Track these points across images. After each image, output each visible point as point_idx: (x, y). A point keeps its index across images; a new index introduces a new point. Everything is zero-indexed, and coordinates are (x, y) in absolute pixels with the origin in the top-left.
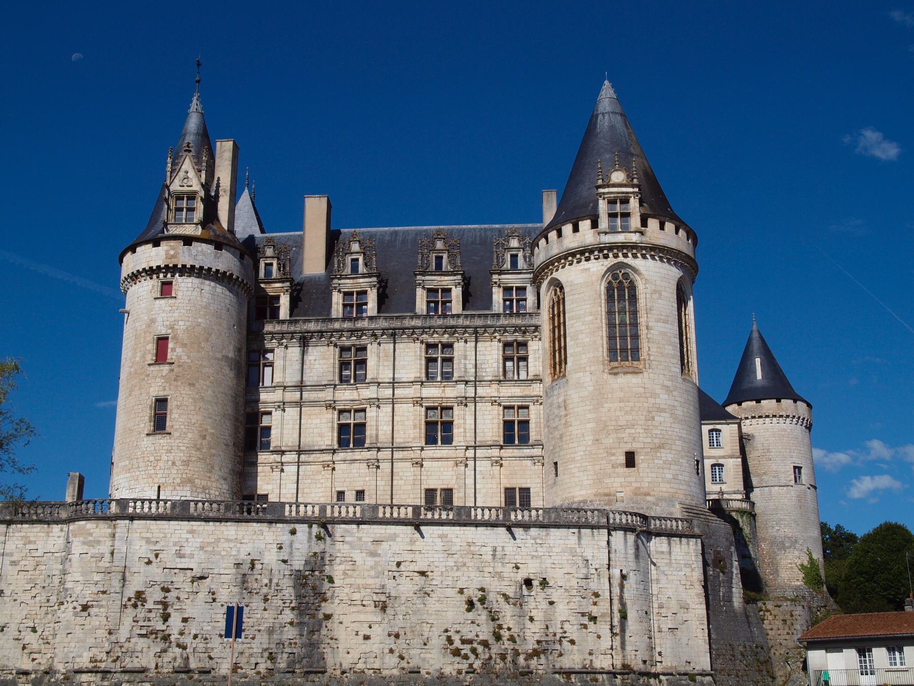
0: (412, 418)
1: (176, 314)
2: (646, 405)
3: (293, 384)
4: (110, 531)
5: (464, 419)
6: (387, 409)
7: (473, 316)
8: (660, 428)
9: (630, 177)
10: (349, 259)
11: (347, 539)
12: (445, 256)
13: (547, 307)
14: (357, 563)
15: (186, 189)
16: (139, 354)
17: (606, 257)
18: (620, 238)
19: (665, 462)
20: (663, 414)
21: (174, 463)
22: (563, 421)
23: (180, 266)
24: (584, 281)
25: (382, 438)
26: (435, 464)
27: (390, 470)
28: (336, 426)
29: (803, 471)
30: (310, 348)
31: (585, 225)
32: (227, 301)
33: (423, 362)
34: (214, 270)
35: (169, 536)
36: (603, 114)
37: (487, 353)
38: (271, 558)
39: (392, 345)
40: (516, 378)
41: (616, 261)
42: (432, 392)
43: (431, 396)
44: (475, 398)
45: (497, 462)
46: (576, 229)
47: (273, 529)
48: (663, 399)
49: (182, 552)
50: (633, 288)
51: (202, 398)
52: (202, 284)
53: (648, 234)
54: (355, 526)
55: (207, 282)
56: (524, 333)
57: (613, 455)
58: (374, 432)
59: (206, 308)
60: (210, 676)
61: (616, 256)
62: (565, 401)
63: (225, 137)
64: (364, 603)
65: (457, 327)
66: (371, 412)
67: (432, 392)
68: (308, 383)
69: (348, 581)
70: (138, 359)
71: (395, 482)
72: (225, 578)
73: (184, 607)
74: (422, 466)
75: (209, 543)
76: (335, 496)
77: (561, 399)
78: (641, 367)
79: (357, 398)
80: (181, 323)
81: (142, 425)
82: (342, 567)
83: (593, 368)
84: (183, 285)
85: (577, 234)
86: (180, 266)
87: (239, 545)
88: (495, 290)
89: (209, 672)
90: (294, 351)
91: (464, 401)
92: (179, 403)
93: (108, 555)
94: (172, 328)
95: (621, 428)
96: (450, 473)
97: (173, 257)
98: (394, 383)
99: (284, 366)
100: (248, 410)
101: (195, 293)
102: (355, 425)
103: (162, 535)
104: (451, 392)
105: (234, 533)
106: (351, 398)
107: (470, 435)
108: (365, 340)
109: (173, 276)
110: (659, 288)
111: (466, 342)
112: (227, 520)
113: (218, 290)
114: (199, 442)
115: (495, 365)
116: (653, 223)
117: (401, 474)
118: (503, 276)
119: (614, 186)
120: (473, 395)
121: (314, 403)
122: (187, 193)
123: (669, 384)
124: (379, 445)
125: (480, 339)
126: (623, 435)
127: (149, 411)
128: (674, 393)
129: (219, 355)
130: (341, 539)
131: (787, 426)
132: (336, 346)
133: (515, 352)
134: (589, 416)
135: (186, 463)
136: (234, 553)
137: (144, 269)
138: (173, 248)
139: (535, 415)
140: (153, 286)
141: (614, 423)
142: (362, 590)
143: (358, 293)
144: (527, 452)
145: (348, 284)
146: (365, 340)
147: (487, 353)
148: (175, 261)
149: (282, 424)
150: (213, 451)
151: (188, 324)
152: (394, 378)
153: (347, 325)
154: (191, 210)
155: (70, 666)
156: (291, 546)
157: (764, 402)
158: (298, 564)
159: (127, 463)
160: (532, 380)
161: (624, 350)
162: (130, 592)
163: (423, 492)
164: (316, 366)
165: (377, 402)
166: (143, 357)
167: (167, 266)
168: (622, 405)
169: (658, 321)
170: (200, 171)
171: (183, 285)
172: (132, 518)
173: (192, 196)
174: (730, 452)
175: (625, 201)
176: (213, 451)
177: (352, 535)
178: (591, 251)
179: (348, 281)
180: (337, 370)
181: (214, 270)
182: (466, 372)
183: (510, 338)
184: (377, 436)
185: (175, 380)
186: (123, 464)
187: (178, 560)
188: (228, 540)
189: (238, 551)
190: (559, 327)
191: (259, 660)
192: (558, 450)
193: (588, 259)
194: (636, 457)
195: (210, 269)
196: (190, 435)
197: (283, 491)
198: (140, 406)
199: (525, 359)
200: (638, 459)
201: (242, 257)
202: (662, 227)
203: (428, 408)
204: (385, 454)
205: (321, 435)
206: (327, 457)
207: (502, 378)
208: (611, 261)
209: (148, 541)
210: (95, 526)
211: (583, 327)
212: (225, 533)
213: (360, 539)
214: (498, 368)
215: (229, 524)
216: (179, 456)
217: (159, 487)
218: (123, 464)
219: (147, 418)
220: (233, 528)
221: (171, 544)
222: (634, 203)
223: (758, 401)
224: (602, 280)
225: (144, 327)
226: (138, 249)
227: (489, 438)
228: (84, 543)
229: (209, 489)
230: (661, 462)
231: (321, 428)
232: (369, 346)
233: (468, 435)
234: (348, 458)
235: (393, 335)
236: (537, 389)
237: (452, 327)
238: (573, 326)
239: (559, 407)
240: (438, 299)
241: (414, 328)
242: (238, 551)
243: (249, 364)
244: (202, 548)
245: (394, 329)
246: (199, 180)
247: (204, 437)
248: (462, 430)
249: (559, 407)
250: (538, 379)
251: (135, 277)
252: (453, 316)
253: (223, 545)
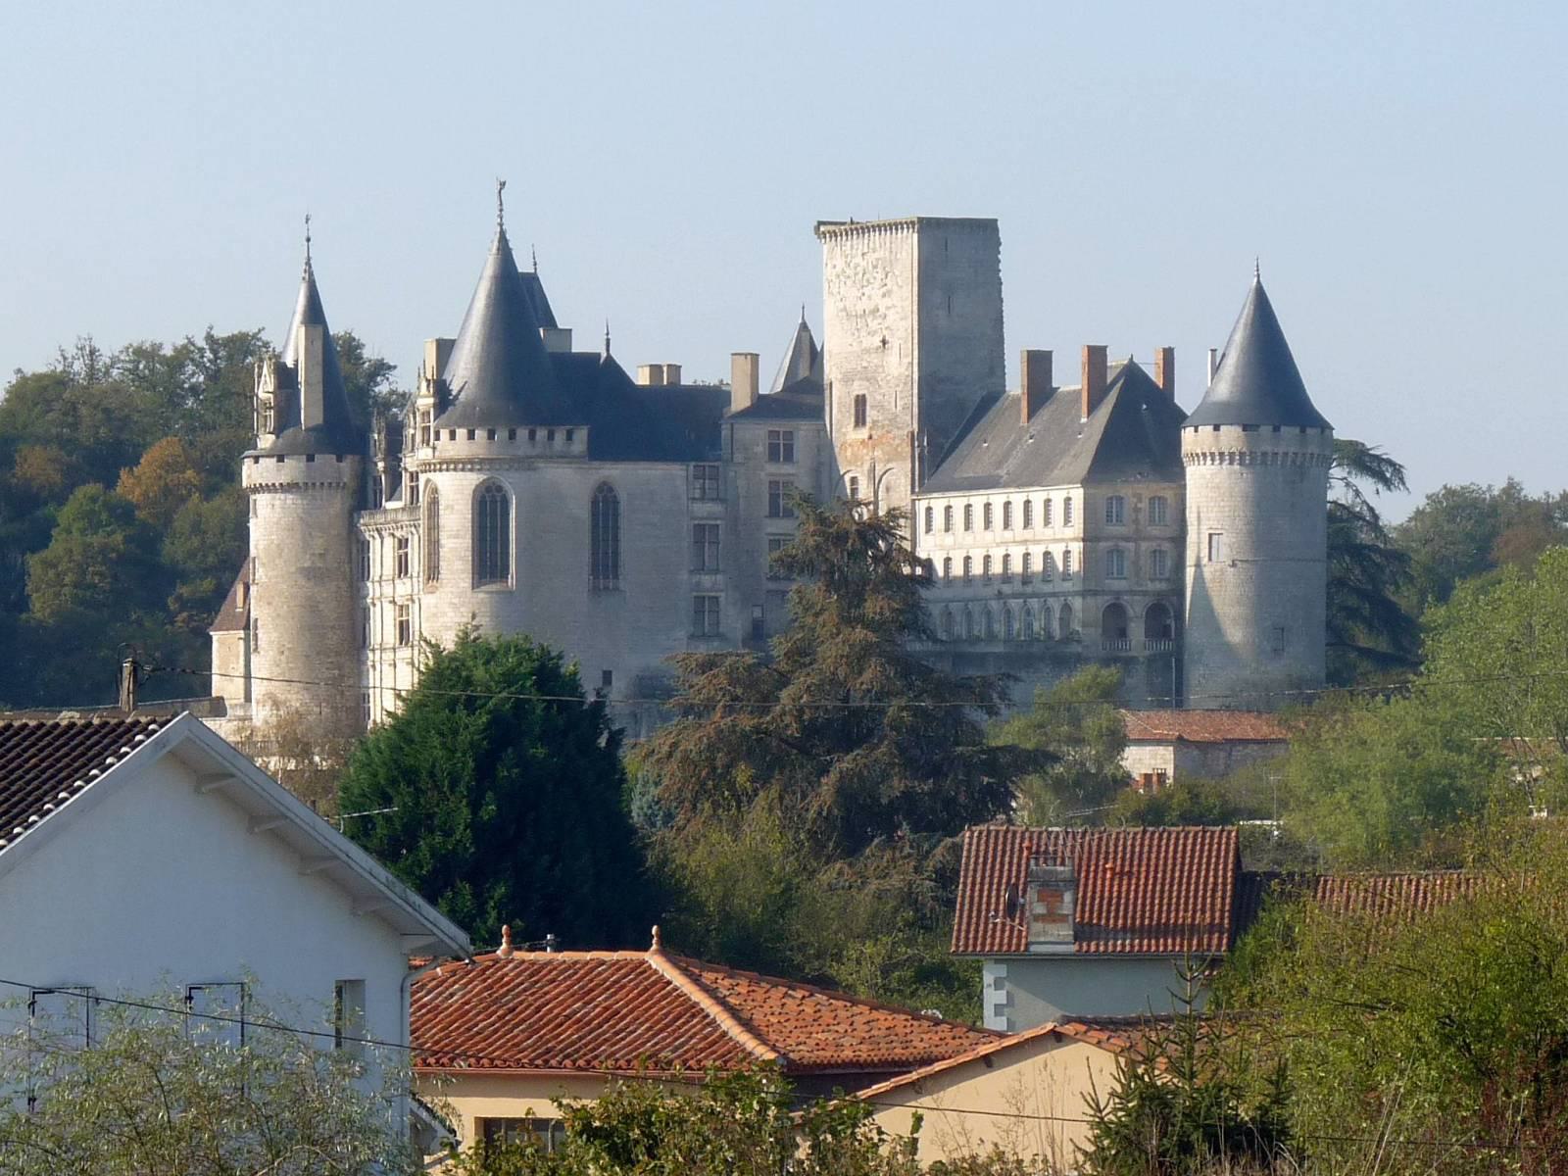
32: (300, 511)
51: (278, 615)
52: (274, 498)
55: (278, 496)
113: (288, 502)
123: (456, 601)
128: (462, 609)
129: (293, 569)
195: (274, 485)
196: (271, 653)
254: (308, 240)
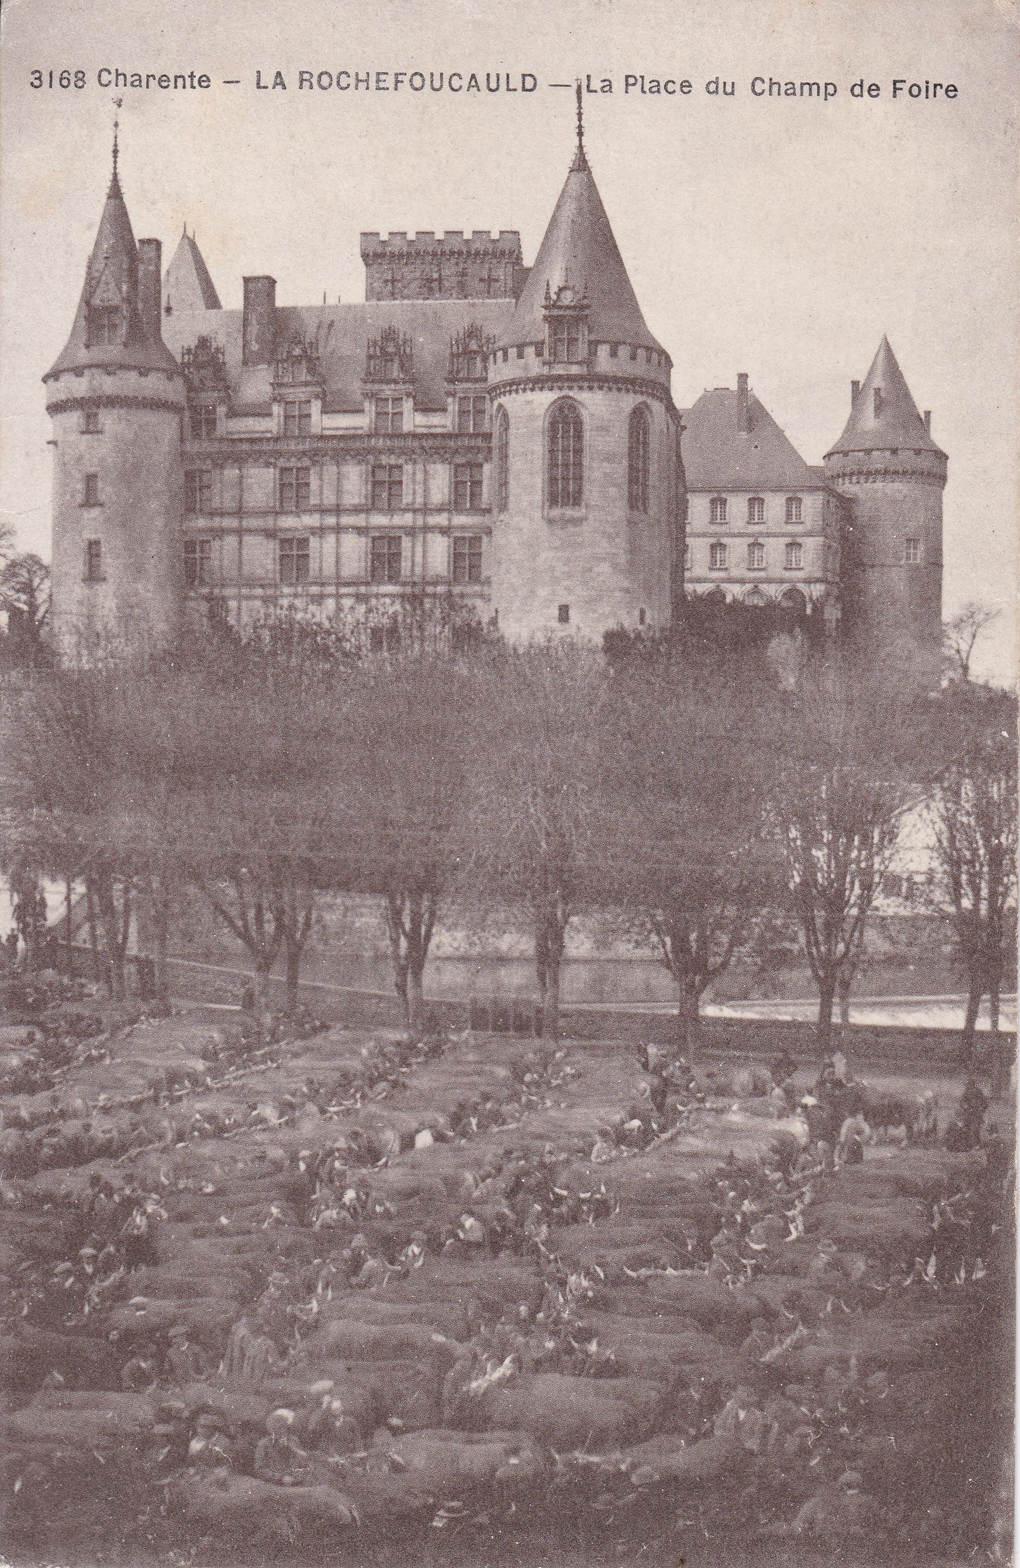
50: (579, 424)
58: (317, 565)
84: (108, 420)
184: (321, 569)
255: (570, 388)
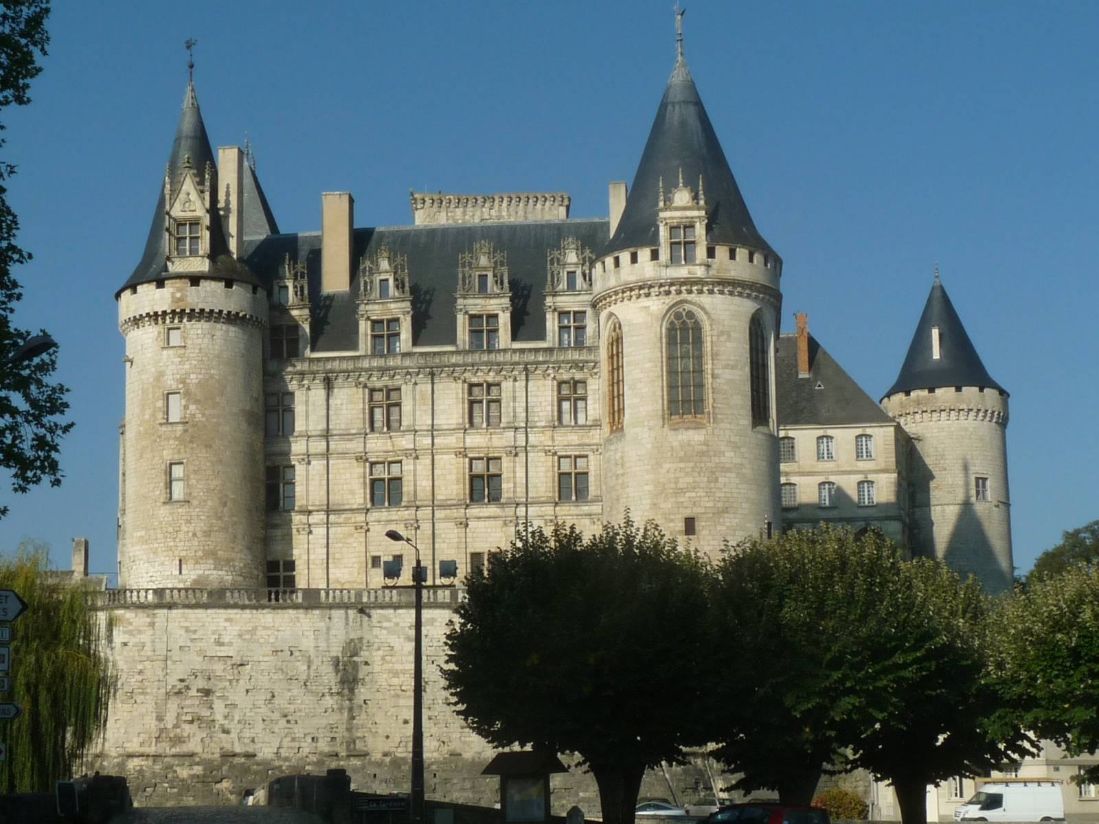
0: (455, 471)
1: (187, 366)
2: (709, 464)
3: (319, 433)
4: (148, 620)
5: (514, 472)
6: (425, 461)
7: (522, 351)
8: (724, 490)
9: (696, 198)
10: (377, 278)
11: (385, 624)
12: (490, 275)
13: (606, 343)
14: (395, 649)
15: (189, 214)
16: (148, 413)
17: (668, 293)
18: (682, 272)
19: (728, 528)
20: (728, 475)
21: (194, 535)
22: (620, 481)
23: (188, 311)
24: (642, 320)
25: (420, 495)
26: (481, 524)
27: (431, 532)
28: (368, 481)
29: (988, 483)
30: (336, 390)
31: (644, 254)
33: (466, 406)
34: (225, 312)
35: (207, 624)
36: (673, 104)
37: (539, 394)
38: (308, 644)
39: (429, 386)
40: (573, 424)
41: (678, 298)
42: (476, 440)
43: (476, 445)
44: (526, 447)
45: (551, 521)
46: (634, 259)
47: (309, 616)
48: (730, 457)
49: (221, 640)
50: (698, 328)
53: (715, 266)
54: (391, 611)
55: (219, 326)
56: (582, 368)
57: (672, 521)
58: (412, 488)
59: (219, 356)
60: (252, 760)
61: (679, 292)
62: (622, 458)
63: (228, 143)
64: (403, 688)
65: (505, 364)
66: (408, 466)
67: (476, 440)
68: (335, 432)
69: (387, 666)
70: (147, 417)
71: (437, 546)
72: (263, 666)
73: (226, 694)
74: (467, 525)
75: (246, 631)
76: (370, 562)
77: (618, 455)
78: (705, 422)
79: (390, 448)
80: (193, 376)
81: (158, 493)
82: (381, 653)
83: (651, 423)
85: (636, 265)
86: (188, 311)
87: (276, 633)
88: (549, 316)
89: (255, 755)
90: (318, 393)
91: (514, 452)
92: (196, 468)
93: (148, 645)
94: (183, 381)
95: (681, 491)
96: (498, 535)
97: (180, 300)
98: (433, 429)
99: (307, 412)
100: (268, 464)
101: (206, 340)
102: (390, 480)
103: (200, 624)
104: (501, 440)
105: (271, 620)
106: (385, 449)
107: (521, 491)
108: (398, 381)
109: (181, 321)
110: (727, 329)
111: (515, 380)
112: (263, 607)
113: (230, 334)
114: (220, 510)
115: (549, 408)
116: (722, 252)
117: (443, 536)
118: (559, 299)
119: (677, 209)
120: (524, 444)
121: (343, 455)
122: (189, 220)
124: (418, 503)
125: (531, 377)
126: (682, 500)
127: (163, 477)
128: (743, 450)
129: (235, 410)
130: (379, 625)
131: (970, 423)
132: (365, 386)
133: (570, 393)
134: (648, 477)
135: (207, 534)
136: (272, 640)
137: (148, 314)
138: (179, 290)
139: (593, 466)
140: (159, 333)
141: (673, 486)
142: (401, 675)
143: (389, 321)
144: (585, 509)
145: (376, 310)
146: (398, 381)
147: (539, 394)
148: (181, 305)
149: (307, 480)
150: (235, 519)
151: (200, 376)
152: (433, 425)
153: (376, 363)
154: (194, 239)
155: (121, 751)
156: (328, 633)
157: (937, 391)
158: (336, 651)
159: (143, 533)
160: (591, 426)
161: (686, 401)
162: (173, 680)
163: (469, 556)
164: (344, 412)
165: (415, 454)
166: (153, 415)
167: (173, 312)
168: (682, 465)
169: (725, 367)
170: (202, 192)
171: (192, 332)
172: (170, 606)
173: (195, 223)
174: (883, 466)
175: (690, 226)
176: (235, 519)
177: (389, 620)
178: (651, 287)
179: (376, 307)
180: (367, 416)
181: (225, 312)
182: (515, 416)
183: (566, 377)
184: (415, 492)
185: (191, 442)
186: (139, 534)
187: (218, 648)
188: (265, 628)
189: (277, 638)
190: (618, 369)
191: (303, 744)
192: (614, 512)
193: (648, 295)
194: (696, 523)
197: (312, 557)
198: (153, 471)
199: (584, 399)
200: (699, 525)
201: (254, 291)
202: (732, 256)
203: (471, 459)
204: (424, 513)
205: (352, 492)
206: (360, 518)
207: (556, 423)
208: (673, 298)
209: (187, 630)
210: (133, 615)
211: (641, 376)
212: (262, 621)
213: (397, 624)
214: (552, 411)
215: (265, 611)
216: (199, 526)
217: (180, 561)
218: (139, 534)
219: (162, 484)
220: (270, 616)
221: (210, 632)
222: (700, 230)
223: (932, 390)
224: (663, 320)
225: (151, 380)
226: (139, 288)
227: (542, 494)
228: (125, 632)
229: (233, 560)
230: (724, 528)
231: (351, 485)
232: (403, 387)
233: (518, 490)
234: (383, 518)
235: (432, 374)
236: (596, 436)
237: (498, 364)
238: (630, 373)
239: (617, 464)
240: (482, 327)
241: (455, 365)
242: (277, 638)
243: (270, 416)
244: (240, 636)
245: (432, 368)
246: (203, 204)
247: (225, 504)
248: (512, 485)
249: (617, 464)
250: (597, 424)
251: (137, 321)
252: (499, 351)
253: (260, 632)
254: (192, 66)
255: (690, 292)
